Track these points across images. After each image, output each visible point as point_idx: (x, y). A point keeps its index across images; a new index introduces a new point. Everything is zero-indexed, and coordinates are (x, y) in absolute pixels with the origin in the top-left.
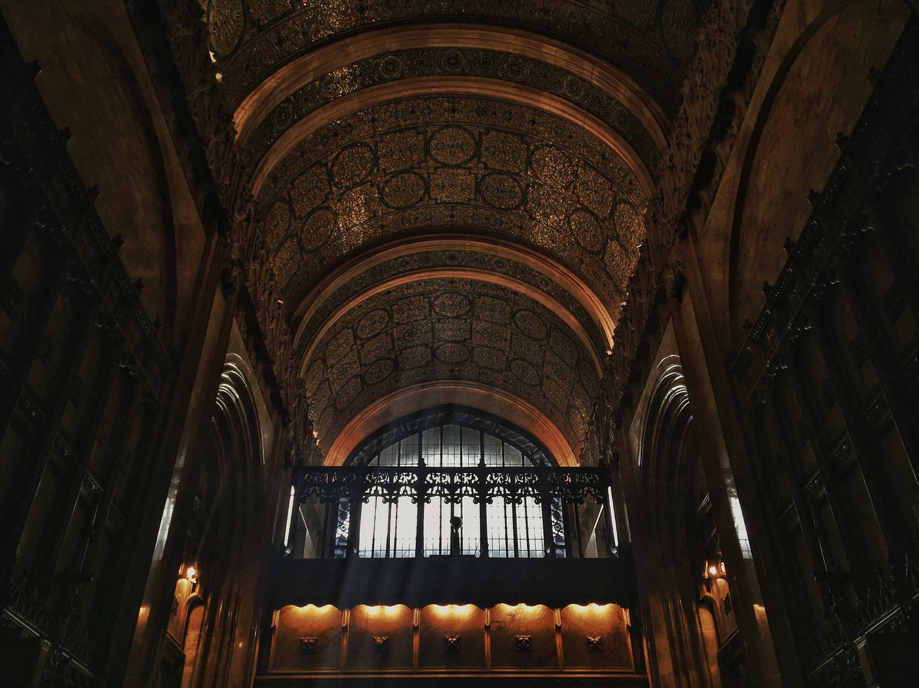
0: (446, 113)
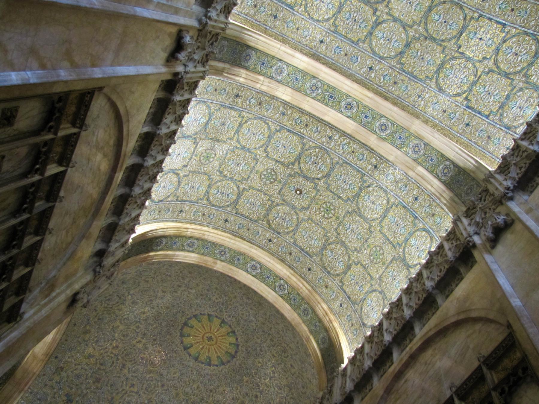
0: (376, 69)
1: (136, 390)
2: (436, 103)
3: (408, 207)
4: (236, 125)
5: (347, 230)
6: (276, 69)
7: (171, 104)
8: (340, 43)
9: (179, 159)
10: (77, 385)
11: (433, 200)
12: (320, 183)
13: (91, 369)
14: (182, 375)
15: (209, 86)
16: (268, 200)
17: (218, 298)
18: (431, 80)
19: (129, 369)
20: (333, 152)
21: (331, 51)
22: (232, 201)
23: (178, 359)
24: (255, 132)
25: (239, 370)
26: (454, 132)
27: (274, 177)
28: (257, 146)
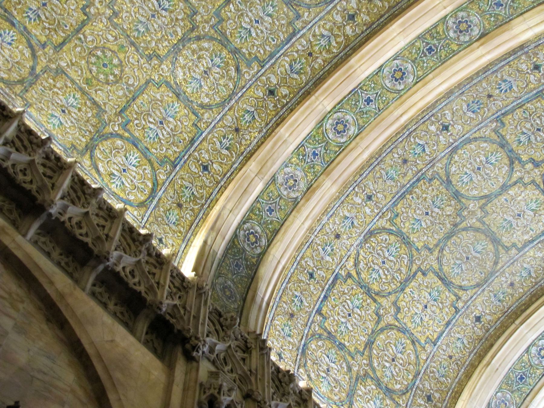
2: (353, 223)
3: (193, 149)
8: (515, 95)
11: (203, 205)
18: (390, 220)
20: (322, 15)
21: (510, 75)
26: (303, 251)
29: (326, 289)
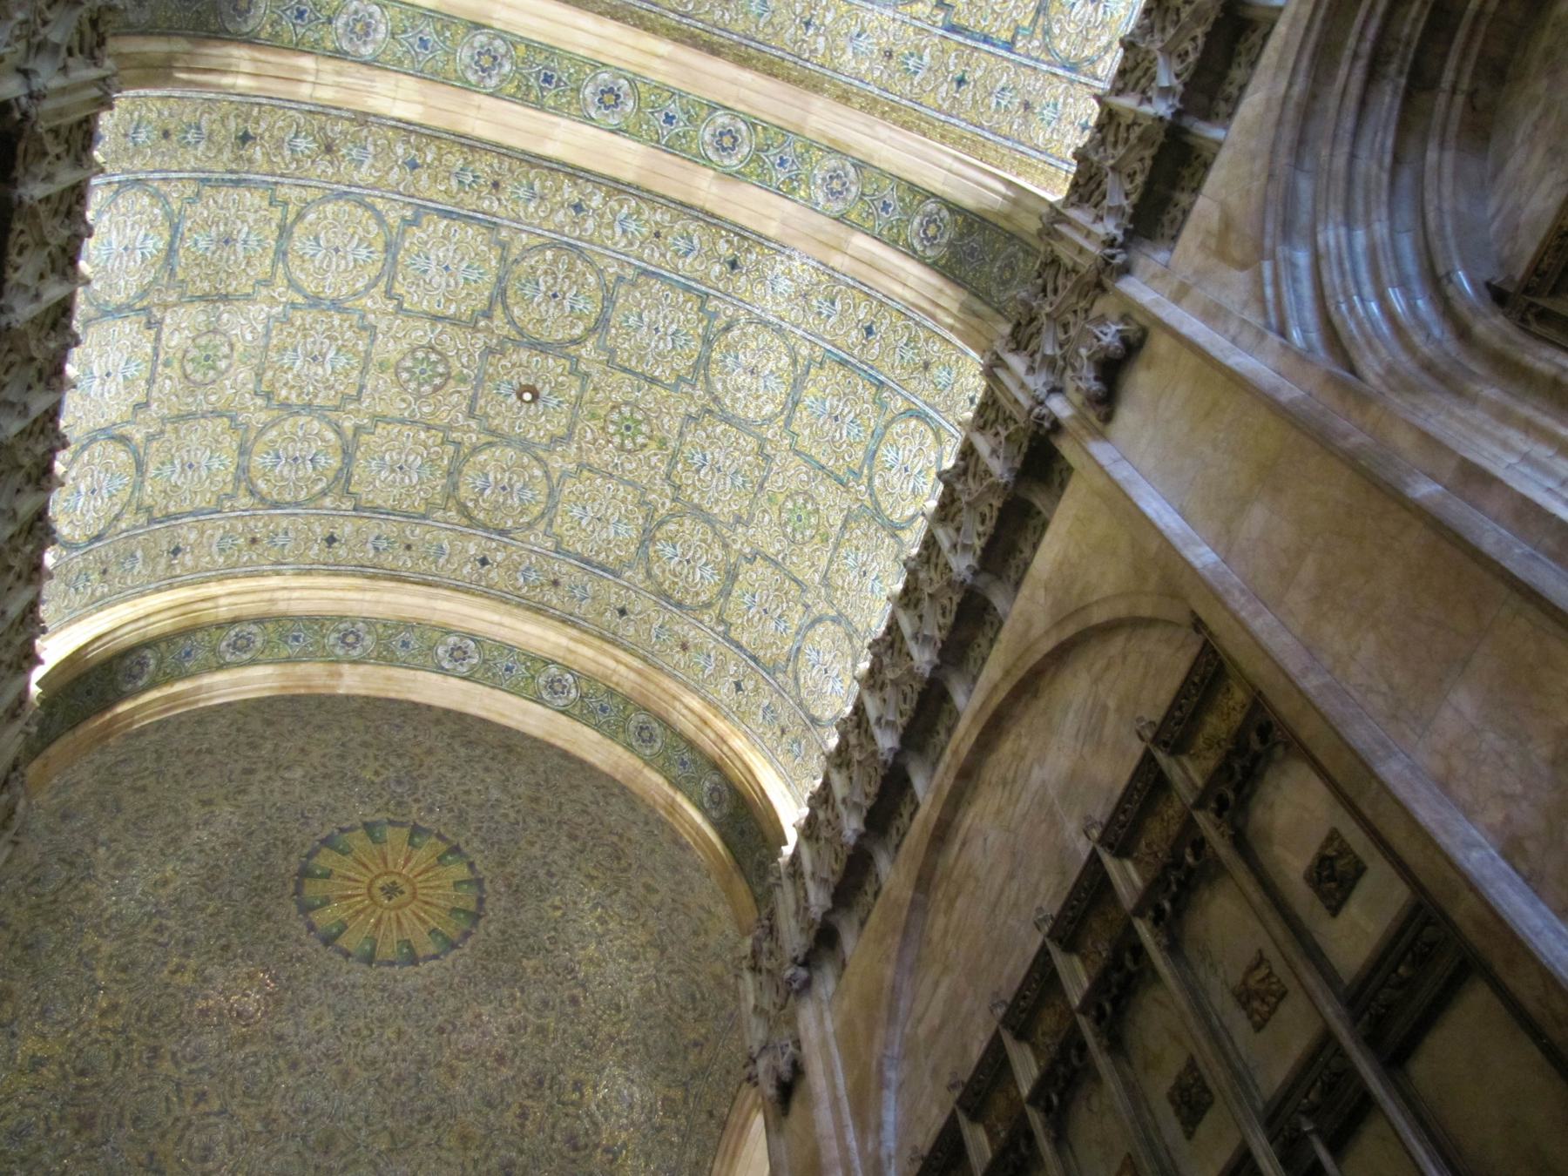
1: (216, 1105)
2: (859, 35)
4: (272, 231)
5: (698, 471)
6: (347, 24)
7: (16, 216)
9: (113, 390)
10: (23, 1160)
11: (917, 324)
12: (583, 351)
13: (54, 1097)
14: (339, 1016)
15: (138, 126)
16: (443, 443)
17: (382, 770)
19: (174, 1054)
22: (331, 474)
23: (316, 975)
24: (338, 243)
25: (504, 949)
26: (929, 112)
27: (441, 369)
28: (360, 285)
29: (973, 44)
